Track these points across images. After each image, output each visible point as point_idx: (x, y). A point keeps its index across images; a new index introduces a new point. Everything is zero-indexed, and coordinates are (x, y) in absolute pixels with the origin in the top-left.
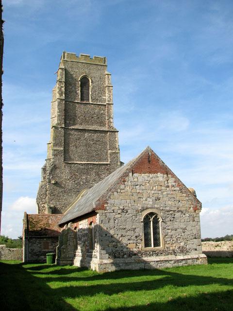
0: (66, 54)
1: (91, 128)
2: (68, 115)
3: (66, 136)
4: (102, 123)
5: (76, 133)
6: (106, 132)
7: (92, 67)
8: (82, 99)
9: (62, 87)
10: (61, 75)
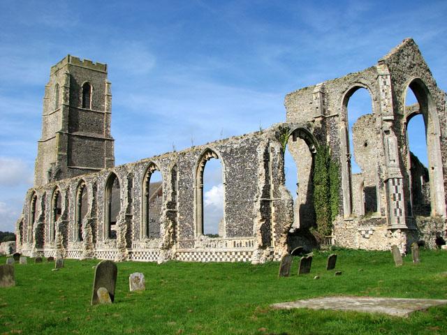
0: (70, 58)
1: (91, 135)
2: (72, 121)
3: (70, 141)
4: (100, 131)
5: (78, 139)
6: (104, 140)
7: (94, 74)
8: (84, 106)
9: (67, 93)
10: (67, 80)
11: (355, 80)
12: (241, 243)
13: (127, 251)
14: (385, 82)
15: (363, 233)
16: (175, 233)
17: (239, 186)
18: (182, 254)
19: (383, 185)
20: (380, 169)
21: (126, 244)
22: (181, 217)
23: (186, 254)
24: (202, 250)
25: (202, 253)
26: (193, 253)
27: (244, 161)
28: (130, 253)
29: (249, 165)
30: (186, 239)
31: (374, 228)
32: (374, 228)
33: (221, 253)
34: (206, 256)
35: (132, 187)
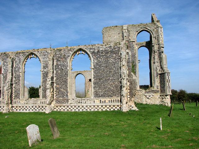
11: (144, 27)
12: (105, 101)
13: (10, 106)
14: (161, 30)
15: (148, 96)
16: (53, 95)
17: (104, 70)
18: (59, 107)
19: (158, 75)
20: (156, 68)
21: (10, 102)
22: (57, 86)
23: (62, 107)
24: (75, 105)
25: (75, 106)
26: (68, 106)
27: (107, 58)
28: (12, 107)
29: (111, 60)
30: (61, 98)
31: (153, 94)
32: (153, 94)
33: (90, 106)
34: (79, 108)
35: (13, 66)
